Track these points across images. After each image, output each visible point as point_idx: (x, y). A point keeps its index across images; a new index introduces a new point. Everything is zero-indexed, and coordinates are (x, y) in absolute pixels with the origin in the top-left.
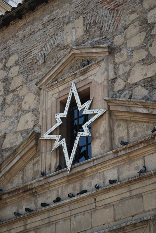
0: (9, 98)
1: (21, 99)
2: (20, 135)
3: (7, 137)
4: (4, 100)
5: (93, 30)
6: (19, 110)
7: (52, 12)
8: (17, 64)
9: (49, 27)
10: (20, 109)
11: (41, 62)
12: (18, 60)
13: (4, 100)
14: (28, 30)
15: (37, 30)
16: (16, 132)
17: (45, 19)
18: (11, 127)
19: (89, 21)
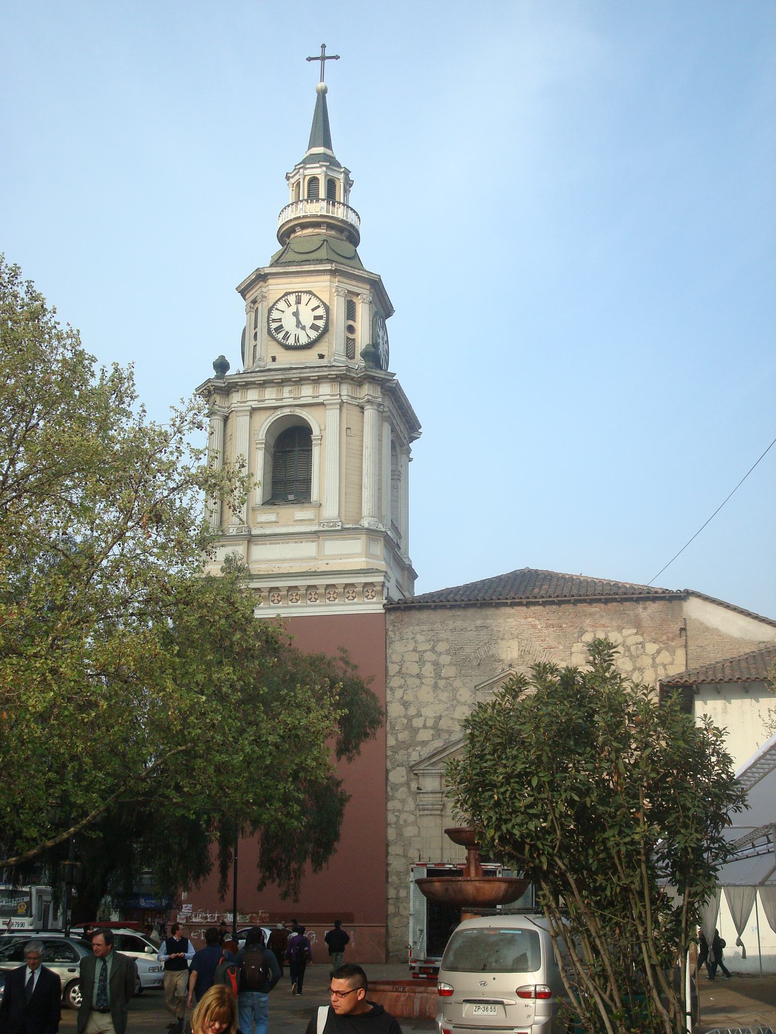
0: (441, 683)
1: (455, 690)
2: (456, 723)
3: (442, 718)
4: (436, 683)
5: (528, 658)
6: (453, 700)
7: (485, 619)
8: (448, 652)
9: (483, 633)
10: (454, 698)
11: (475, 663)
12: (449, 650)
13: (436, 683)
14: (459, 623)
15: (469, 629)
16: (452, 719)
17: (479, 623)
18: (447, 713)
19: (522, 648)
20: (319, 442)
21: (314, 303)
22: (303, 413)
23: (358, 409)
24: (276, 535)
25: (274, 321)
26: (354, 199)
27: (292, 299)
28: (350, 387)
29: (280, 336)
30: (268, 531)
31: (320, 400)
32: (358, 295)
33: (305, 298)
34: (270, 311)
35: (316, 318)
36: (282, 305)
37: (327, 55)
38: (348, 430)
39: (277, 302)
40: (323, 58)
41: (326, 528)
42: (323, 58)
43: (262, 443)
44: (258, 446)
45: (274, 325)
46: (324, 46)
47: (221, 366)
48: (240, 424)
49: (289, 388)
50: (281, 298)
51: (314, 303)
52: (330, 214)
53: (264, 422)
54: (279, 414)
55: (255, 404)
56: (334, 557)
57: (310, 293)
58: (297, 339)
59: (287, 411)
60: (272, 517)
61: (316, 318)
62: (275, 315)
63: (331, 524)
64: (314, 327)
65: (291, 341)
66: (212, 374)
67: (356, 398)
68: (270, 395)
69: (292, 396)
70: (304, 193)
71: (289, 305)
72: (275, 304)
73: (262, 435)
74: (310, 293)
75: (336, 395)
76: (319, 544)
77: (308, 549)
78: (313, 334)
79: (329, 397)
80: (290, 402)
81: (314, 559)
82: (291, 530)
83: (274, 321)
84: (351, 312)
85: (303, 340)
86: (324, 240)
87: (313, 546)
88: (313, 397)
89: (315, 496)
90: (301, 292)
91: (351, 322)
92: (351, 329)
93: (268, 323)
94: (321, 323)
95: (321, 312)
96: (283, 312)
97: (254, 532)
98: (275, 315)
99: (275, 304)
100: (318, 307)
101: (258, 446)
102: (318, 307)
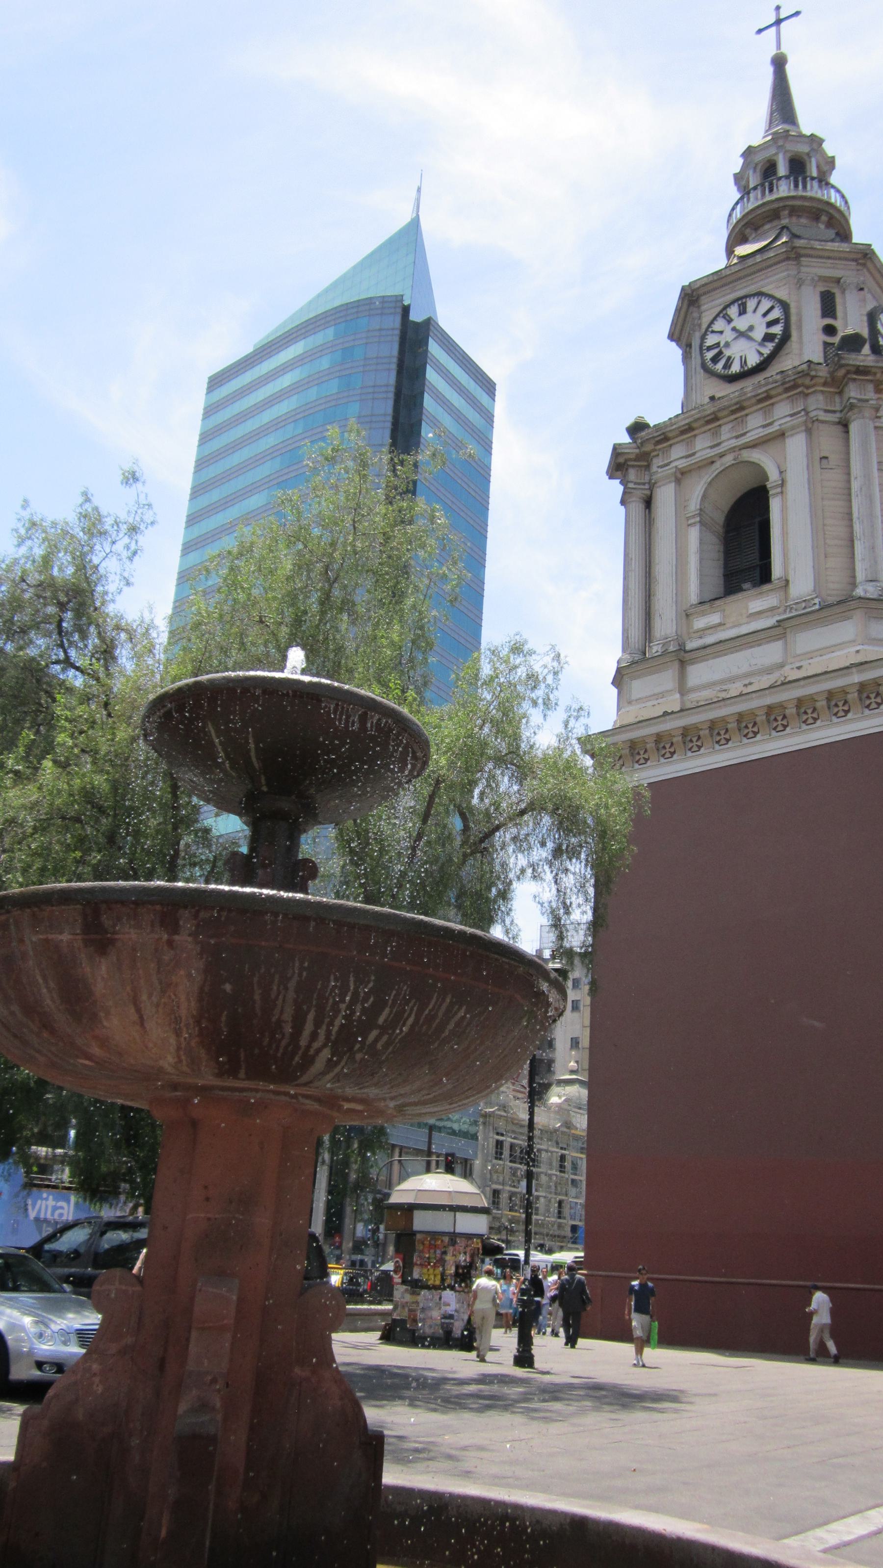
20: (779, 490)
21: (766, 304)
22: (755, 456)
23: (840, 428)
24: (721, 642)
25: (709, 348)
26: (834, 179)
27: (733, 311)
28: (821, 397)
29: (719, 366)
30: (710, 639)
31: (775, 428)
32: (838, 281)
33: (751, 304)
34: (703, 338)
35: (770, 324)
36: (720, 325)
37: (782, 17)
38: (824, 461)
39: (712, 322)
40: (778, 22)
41: (794, 613)
42: (778, 22)
43: (693, 517)
44: (691, 521)
45: (710, 355)
46: (778, 8)
47: (637, 428)
48: (665, 496)
49: (730, 426)
50: (718, 315)
51: (766, 304)
52: (793, 194)
53: (697, 489)
54: (718, 466)
55: (682, 464)
56: (810, 655)
57: (760, 294)
58: (743, 362)
59: (729, 460)
60: (715, 618)
61: (770, 324)
62: (711, 340)
63: (803, 605)
64: (768, 338)
65: (736, 368)
66: (626, 439)
67: (834, 412)
68: (702, 445)
69: (734, 435)
70: (754, 180)
71: (730, 321)
72: (709, 326)
73: (694, 505)
74: (760, 294)
75: (799, 412)
76: (786, 644)
77: (771, 653)
78: (767, 350)
79: (788, 419)
80: (734, 443)
81: (782, 666)
82: (744, 630)
83: (709, 348)
84: (828, 306)
85: (753, 360)
86: (783, 228)
87: (778, 646)
88: (764, 426)
89: (777, 570)
90: (746, 297)
91: (828, 321)
92: (830, 330)
93: (702, 354)
94: (777, 329)
95: (776, 314)
96: (721, 332)
97: (689, 646)
98: (711, 340)
99: (709, 326)
100: (772, 308)
101: (691, 521)
102: (772, 308)
